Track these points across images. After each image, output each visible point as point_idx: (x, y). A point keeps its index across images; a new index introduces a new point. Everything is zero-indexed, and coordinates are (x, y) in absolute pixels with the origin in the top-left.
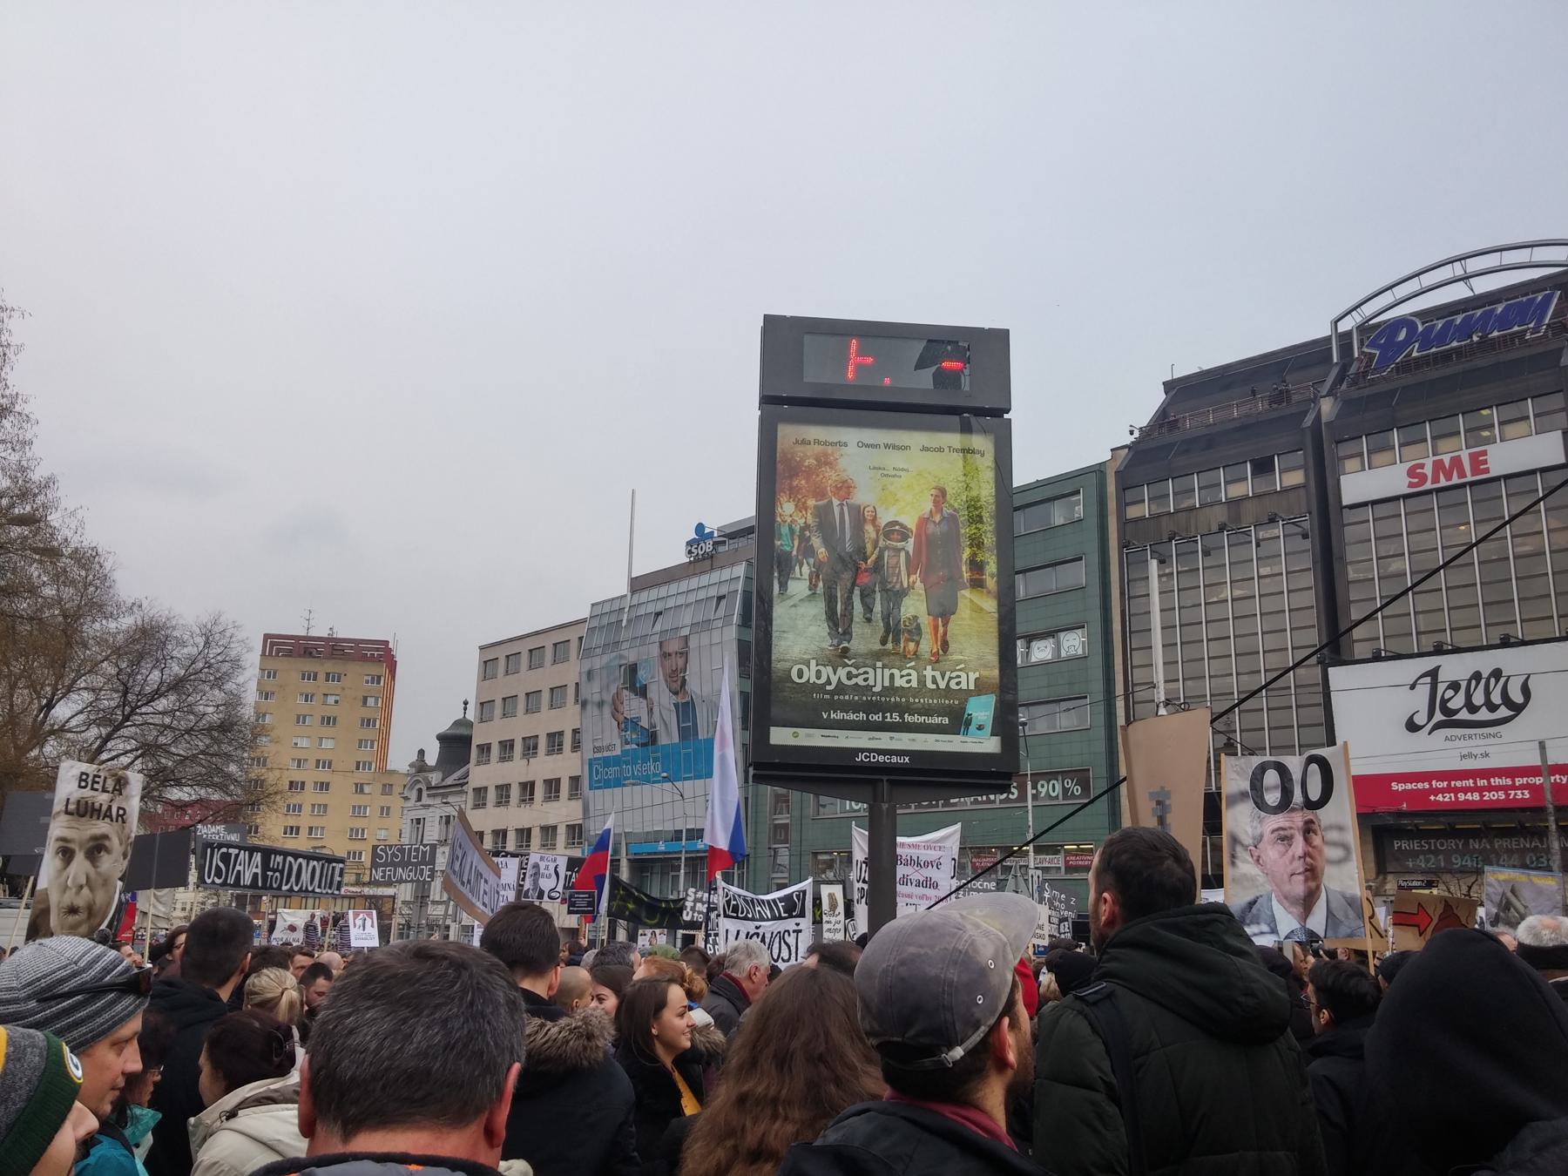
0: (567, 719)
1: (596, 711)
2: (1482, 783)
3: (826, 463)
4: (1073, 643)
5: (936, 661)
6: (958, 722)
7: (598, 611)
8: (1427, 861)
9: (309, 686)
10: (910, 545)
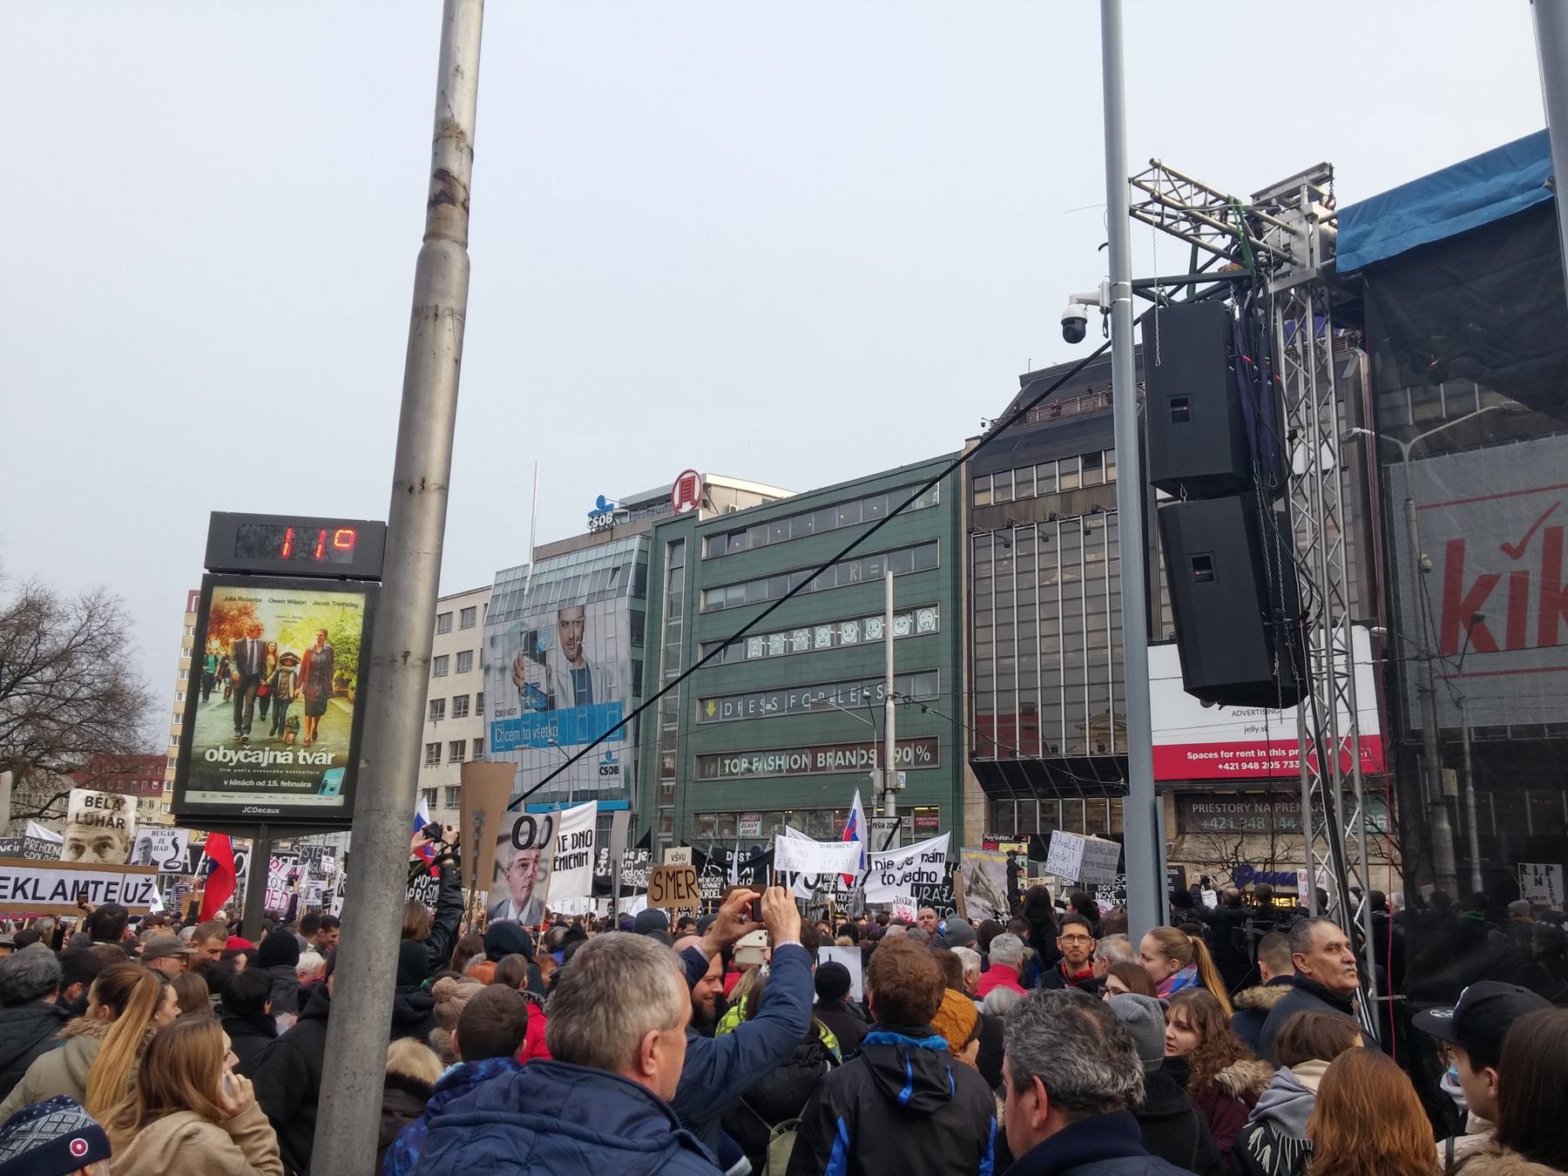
0: (470, 683)
1: (498, 676)
2: (1262, 753)
3: (247, 614)
4: (928, 620)
5: (308, 746)
6: (318, 785)
7: (502, 579)
8: (1219, 823)
10: (298, 669)
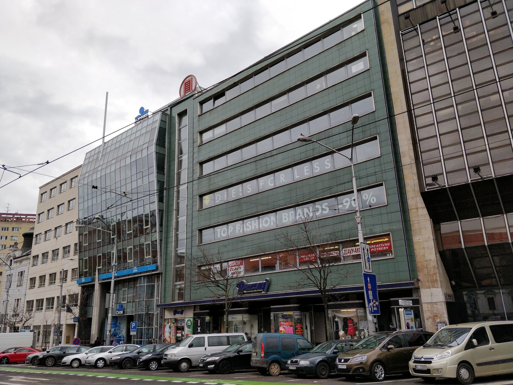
7: (88, 156)
9: (5, 233)
